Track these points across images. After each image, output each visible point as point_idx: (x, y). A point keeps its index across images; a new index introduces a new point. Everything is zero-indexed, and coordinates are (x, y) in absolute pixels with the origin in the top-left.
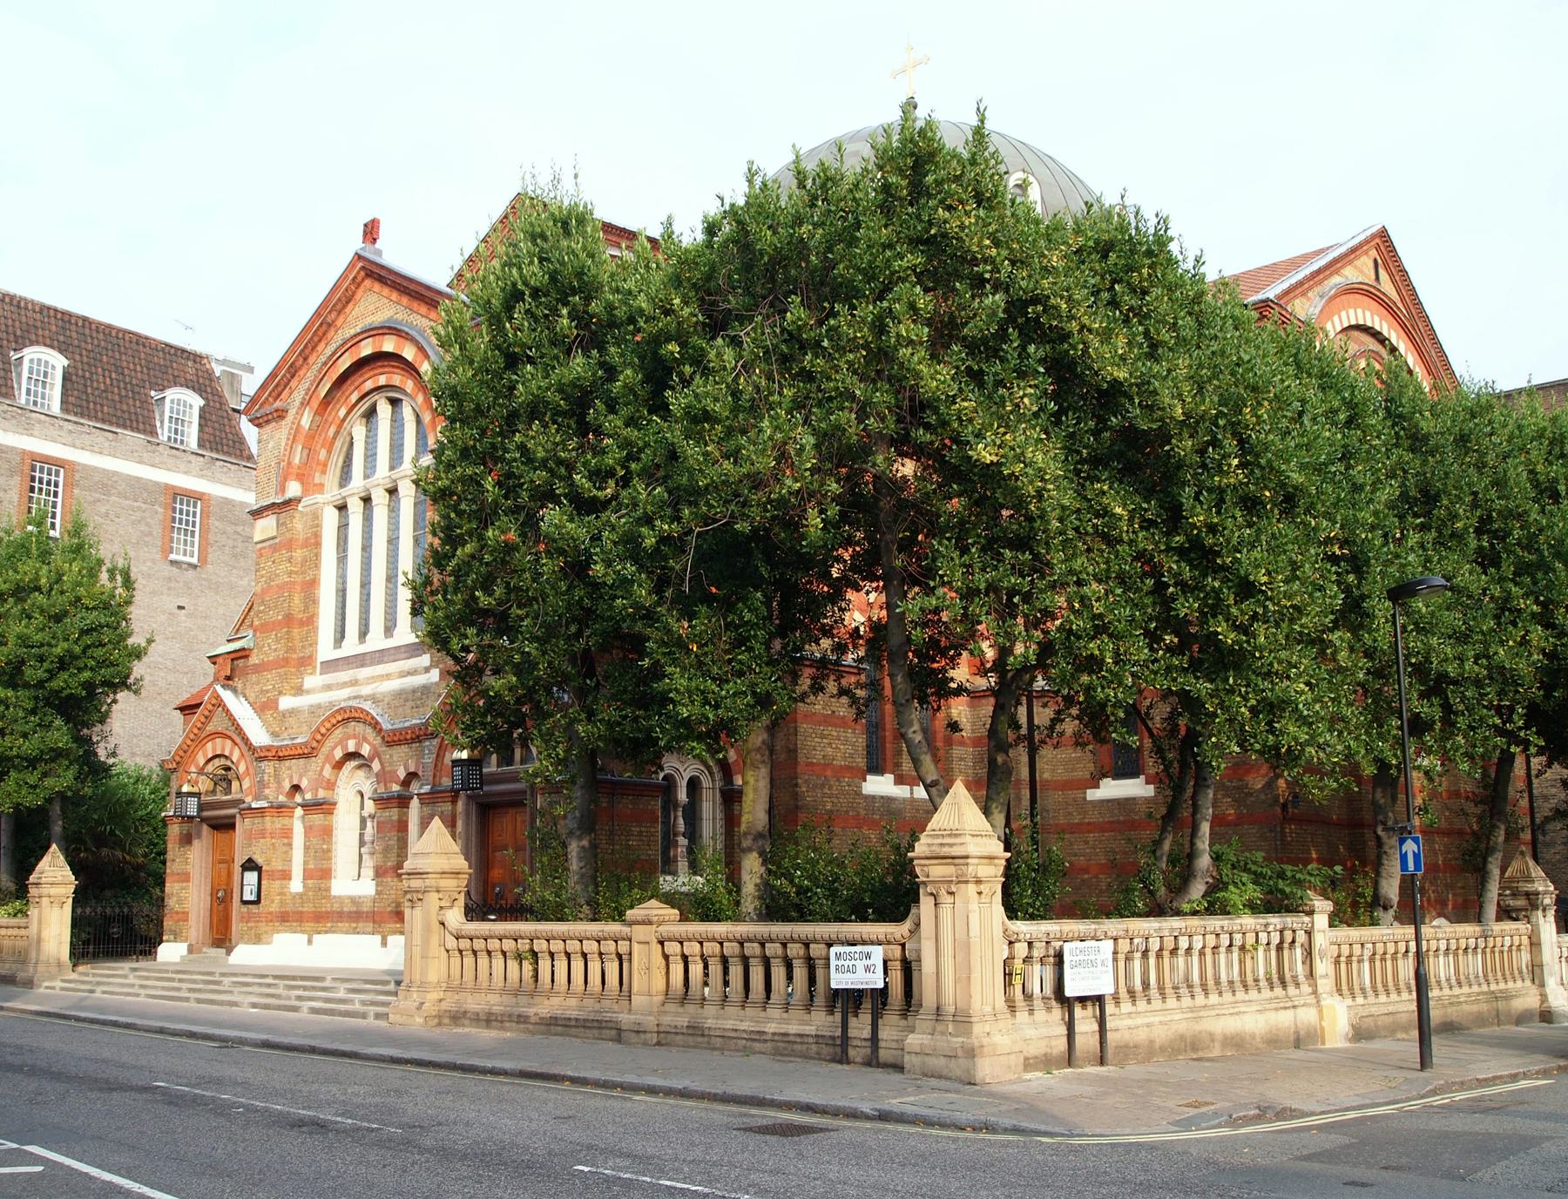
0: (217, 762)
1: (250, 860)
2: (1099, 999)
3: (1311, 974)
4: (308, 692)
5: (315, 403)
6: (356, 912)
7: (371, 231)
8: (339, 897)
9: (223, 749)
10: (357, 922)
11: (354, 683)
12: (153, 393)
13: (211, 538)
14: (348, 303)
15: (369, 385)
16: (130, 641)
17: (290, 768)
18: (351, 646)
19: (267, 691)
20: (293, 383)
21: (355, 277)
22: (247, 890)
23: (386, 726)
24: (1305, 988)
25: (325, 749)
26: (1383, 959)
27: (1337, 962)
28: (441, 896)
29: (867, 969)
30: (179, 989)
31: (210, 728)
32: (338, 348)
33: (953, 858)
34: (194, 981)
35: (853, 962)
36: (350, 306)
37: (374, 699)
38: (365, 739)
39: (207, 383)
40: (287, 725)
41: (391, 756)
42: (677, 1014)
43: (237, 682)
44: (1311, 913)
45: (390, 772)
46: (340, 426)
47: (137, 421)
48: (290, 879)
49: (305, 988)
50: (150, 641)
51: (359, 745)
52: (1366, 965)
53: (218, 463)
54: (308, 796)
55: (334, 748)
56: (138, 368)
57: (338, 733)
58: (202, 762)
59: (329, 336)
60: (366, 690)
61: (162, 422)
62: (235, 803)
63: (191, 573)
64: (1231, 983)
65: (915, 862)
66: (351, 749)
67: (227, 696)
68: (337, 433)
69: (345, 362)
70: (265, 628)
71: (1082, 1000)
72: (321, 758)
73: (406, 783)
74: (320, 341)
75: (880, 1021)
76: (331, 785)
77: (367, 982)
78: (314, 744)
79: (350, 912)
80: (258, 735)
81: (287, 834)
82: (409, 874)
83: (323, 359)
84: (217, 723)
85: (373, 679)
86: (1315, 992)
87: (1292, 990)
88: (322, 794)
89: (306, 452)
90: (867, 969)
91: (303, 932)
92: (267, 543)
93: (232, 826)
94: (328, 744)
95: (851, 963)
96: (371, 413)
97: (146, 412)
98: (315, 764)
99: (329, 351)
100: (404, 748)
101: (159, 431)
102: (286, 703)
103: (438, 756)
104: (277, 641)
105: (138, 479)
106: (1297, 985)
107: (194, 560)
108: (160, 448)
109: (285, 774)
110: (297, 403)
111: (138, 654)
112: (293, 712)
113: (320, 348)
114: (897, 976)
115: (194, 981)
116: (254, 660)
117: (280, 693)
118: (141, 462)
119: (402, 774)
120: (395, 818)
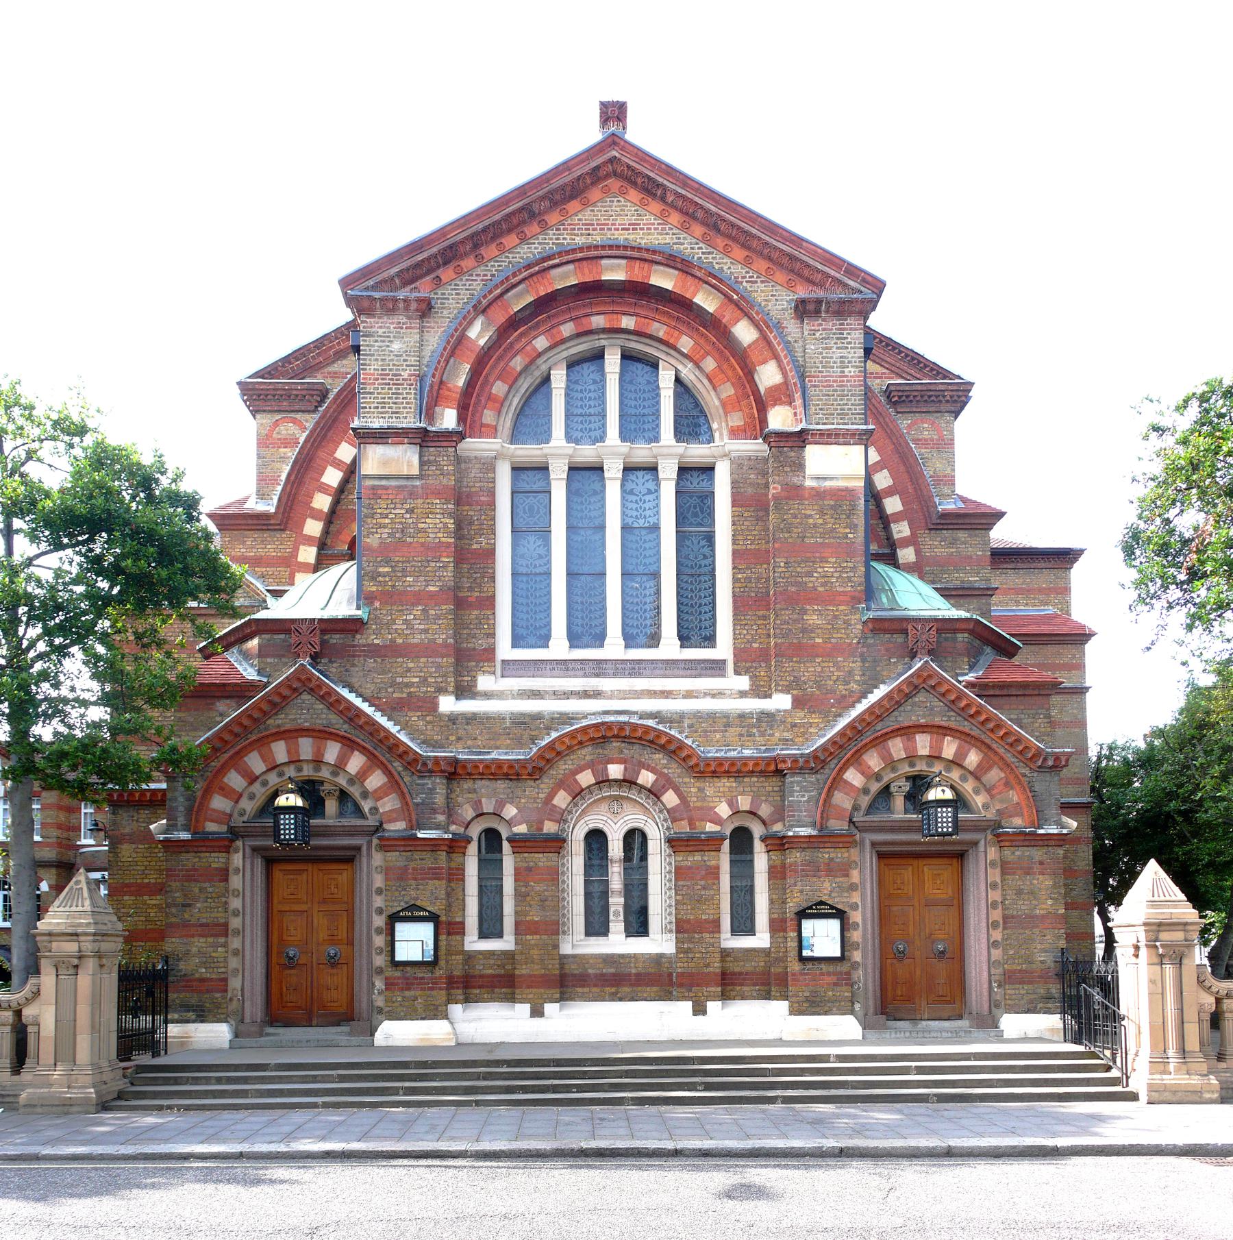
4: (488, 695)
5: (501, 318)
6: (614, 975)
8: (574, 956)
15: (598, 321)
40: (461, 733)
41: (701, 790)
45: (700, 808)
46: (532, 362)
55: (581, 769)
57: (587, 753)
68: (526, 369)
78: (541, 764)
79: (603, 975)
81: (714, 873)
88: (550, 827)
92: (393, 483)
98: (533, 792)
102: (448, 704)
117: (442, 690)
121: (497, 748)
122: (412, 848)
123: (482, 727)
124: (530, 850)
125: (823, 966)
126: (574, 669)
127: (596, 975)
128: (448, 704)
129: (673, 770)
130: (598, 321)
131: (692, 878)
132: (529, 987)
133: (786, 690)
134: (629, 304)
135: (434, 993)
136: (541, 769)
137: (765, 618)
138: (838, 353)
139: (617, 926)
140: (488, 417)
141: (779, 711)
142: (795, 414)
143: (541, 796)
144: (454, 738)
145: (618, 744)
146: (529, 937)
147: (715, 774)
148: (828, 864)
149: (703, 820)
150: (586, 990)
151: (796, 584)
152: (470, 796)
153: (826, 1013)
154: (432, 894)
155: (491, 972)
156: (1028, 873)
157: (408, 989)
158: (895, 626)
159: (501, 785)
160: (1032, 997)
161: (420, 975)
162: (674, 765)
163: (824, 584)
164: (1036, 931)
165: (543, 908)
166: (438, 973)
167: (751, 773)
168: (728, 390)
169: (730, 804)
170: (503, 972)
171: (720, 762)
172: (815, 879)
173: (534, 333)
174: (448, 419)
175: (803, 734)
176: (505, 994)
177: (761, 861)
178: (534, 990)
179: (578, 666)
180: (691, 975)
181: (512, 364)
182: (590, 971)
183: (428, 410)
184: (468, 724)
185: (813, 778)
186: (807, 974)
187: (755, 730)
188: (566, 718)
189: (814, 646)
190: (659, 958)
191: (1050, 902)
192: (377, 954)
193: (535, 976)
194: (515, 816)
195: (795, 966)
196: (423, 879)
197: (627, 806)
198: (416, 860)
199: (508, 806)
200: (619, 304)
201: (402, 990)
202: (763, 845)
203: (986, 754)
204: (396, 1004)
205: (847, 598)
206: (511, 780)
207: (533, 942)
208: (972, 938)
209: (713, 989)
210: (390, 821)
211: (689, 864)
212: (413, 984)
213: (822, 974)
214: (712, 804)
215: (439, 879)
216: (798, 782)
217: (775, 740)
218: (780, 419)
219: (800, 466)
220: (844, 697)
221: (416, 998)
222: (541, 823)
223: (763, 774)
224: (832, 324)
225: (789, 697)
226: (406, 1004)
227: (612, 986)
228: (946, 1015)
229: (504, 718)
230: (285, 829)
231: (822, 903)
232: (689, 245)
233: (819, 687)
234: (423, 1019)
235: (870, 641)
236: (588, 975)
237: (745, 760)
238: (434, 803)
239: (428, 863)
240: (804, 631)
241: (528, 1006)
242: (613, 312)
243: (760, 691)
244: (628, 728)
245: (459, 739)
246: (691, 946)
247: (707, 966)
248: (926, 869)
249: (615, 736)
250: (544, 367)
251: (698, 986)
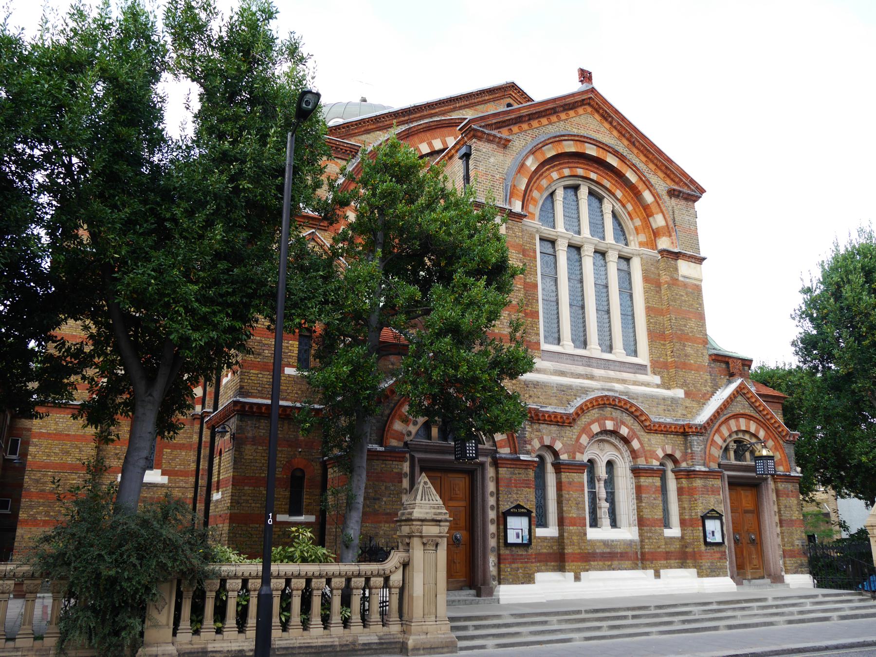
4: (539, 371)
6: (610, 553)
15: (580, 172)
17: (539, 431)
38: (623, 423)
40: (531, 393)
41: (649, 440)
45: (650, 451)
55: (593, 422)
57: (595, 413)
69: (569, 146)
79: (604, 553)
98: (571, 433)
121: (550, 404)
122: (514, 466)
123: (542, 390)
124: (570, 471)
125: (714, 548)
126: (577, 360)
127: (600, 553)
130: (580, 172)
131: (649, 493)
132: (573, 561)
133: (681, 387)
134: (594, 167)
135: (528, 565)
137: (664, 345)
138: (687, 218)
139: (606, 521)
141: (679, 398)
142: (673, 243)
143: (574, 437)
144: (527, 396)
145: (609, 409)
146: (571, 528)
147: (656, 432)
148: (711, 488)
149: (651, 458)
150: (596, 563)
151: (680, 330)
152: (537, 433)
153: (718, 576)
154: (525, 497)
155: (545, 551)
156: (788, 497)
157: (514, 563)
158: (723, 359)
159: (554, 428)
160: (796, 565)
161: (520, 553)
162: (636, 424)
163: (692, 332)
164: (794, 528)
165: (578, 509)
166: (530, 551)
167: (671, 433)
168: (638, 222)
169: (663, 450)
170: (552, 551)
171: (660, 424)
172: (707, 496)
173: (552, 170)
175: (691, 412)
176: (554, 566)
177: (672, 484)
178: (575, 563)
179: (579, 359)
180: (652, 553)
181: (542, 183)
182: (597, 551)
184: (535, 388)
185: (701, 438)
186: (708, 553)
187: (670, 408)
188: (585, 391)
189: (691, 364)
190: (630, 543)
191: (797, 512)
192: (493, 538)
193: (575, 554)
194: (561, 449)
195: (703, 548)
196: (520, 487)
197: (607, 446)
198: (516, 474)
199: (557, 441)
200: (591, 166)
201: (510, 563)
202: (673, 474)
203: (766, 432)
204: (507, 573)
205: (701, 341)
206: (558, 425)
207: (573, 531)
208: (768, 532)
209: (662, 562)
210: (501, 447)
211: (647, 484)
212: (516, 559)
213: (714, 552)
214: (655, 449)
215: (529, 487)
216: (696, 440)
217: (679, 414)
218: (664, 243)
219: (676, 269)
220: (705, 394)
221: (518, 569)
222: (574, 454)
223: (676, 433)
224: (683, 202)
225: (683, 391)
226: (513, 573)
227: (608, 560)
228: (757, 577)
229: (553, 387)
230: (469, 450)
231: (713, 510)
232: (622, 146)
233: (695, 387)
234: (522, 583)
235: (712, 365)
236: (596, 553)
237: (665, 425)
238: (525, 437)
239: (523, 477)
240: (686, 356)
241: (573, 574)
242: (587, 169)
243: (665, 385)
244: (617, 400)
245: (530, 396)
246: (651, 535)
247: (659, 547)
248: (742, 492)
249: (610, 404)
250: (554, 188)
251: (656, 560)
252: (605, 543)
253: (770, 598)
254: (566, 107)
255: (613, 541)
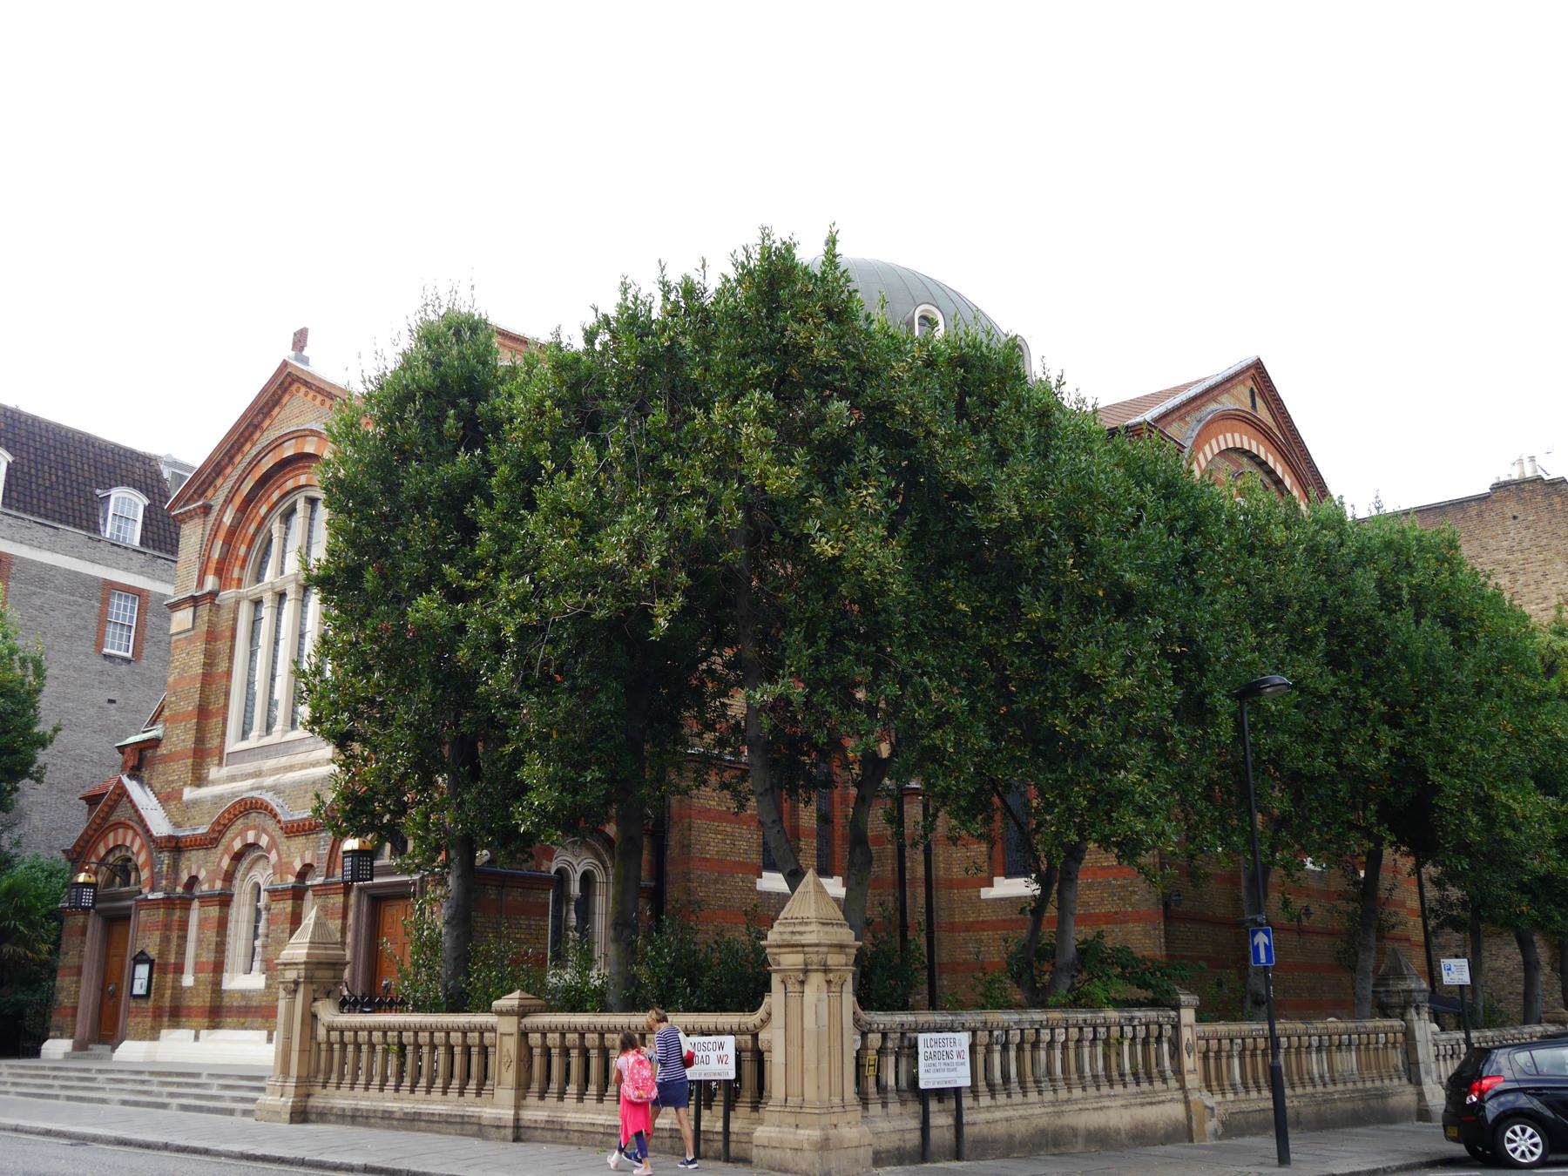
0: (118, 854)
1: (142, 953)
2: (957, 1092)
3: (1179, 1071)
4: (213, 783)
5: (238, 501)
7: (300, 339)
8: (230, 991)
9: (124, 840)
10: (245, 1017)
11: (258, 774)
12: (98, 491)
13: (148, 633)
14: (274, 406)
15: (290, 484)
16: (36, 730)
18: (254, 741)
19: (173, 782)
20: (219, 482)
21: (282, 383)
22: (137, 983)
23: (283, 818)
24: (1173, 1083)
25: (224, 841)
26: (1253, 1055)
27: (1205, 1057)
28: (315, 987)
29: (720, 1060)
30: (51, 1087)
31: (113, 819)
32: (263, 449)
33: (803, 946)
34: (69, 1079)
35: (707, 1053)
36: (277, 409)
37: (276, 789)
38: (264, 831)
39: (155, 483)
41: (289, 847)
42: (538, 1108)
43: (145, 774)
44: (1177, 1007)
47: (81, 519)
48: (182, 973)
49: (179, 1085)
50: (56, 730)
51: (258, 836)
52: (1236, 1061)
53: (159, 561)
54: (205, 887)
55: (233, 839)
56: (86, 467)
57: (239, 824)
58: (102, 852)
59: (256, 436)
60: (269, 781)
61: (105, 520)
62: (130, 896)
63: (124, 668)
64: (1095, 1077)
65: (768, 950)
66: (250, 840)
67: (132, 787)
70: (175, 719)
71: (940, 1094)
72: (221, 847)
73: (302, 875)
74: (246, 441)
75: (732, 1114)
76: (229, 877)
77: (242, 1078)
79: (239, 1007)
80: (160, 825)
82: (285, 964)
83: (248, 458)
84: (120, 814)
85: (276, 771)
86: (1183, 1088)
87: (1158, 1085)
89: (226, 546)
90: (720, 1060)
91: (191, 1028)
92: (183, 636)
93: (128, 918)
94: (229, 835)
95: (704, 1054)
96: (292, 511)
97: (90, 510)
99: (254, 452)
100: (301, 840)
101: (102, 528)
102: (189, 794)
103: (333, 847)
104: (186, 731)
105: (76, 574)
106: (1165, 1080)
107: (129, 655)
108: (101, 545)
109: (184, 864)
110: (221, 501)
111: (43, 742)
112: (195, 803)
113: (247, 447)
114: (748, 1067)
115: (69, 1079)
116: (162, 750)
117: (185, 784)
118: (80, 558)
119: (298, 866)
120: (289, 909)
128: (189, 794)
129: (277, 833)
136: (216, 839)
140: (236, 574)
159: (201, 853)
166: (150, 1003)
174: (211, 582)
183: (201, 583)
252: (243, 994)
253: (205, 1074)
254: (265, 410)
255: (250, 991)
